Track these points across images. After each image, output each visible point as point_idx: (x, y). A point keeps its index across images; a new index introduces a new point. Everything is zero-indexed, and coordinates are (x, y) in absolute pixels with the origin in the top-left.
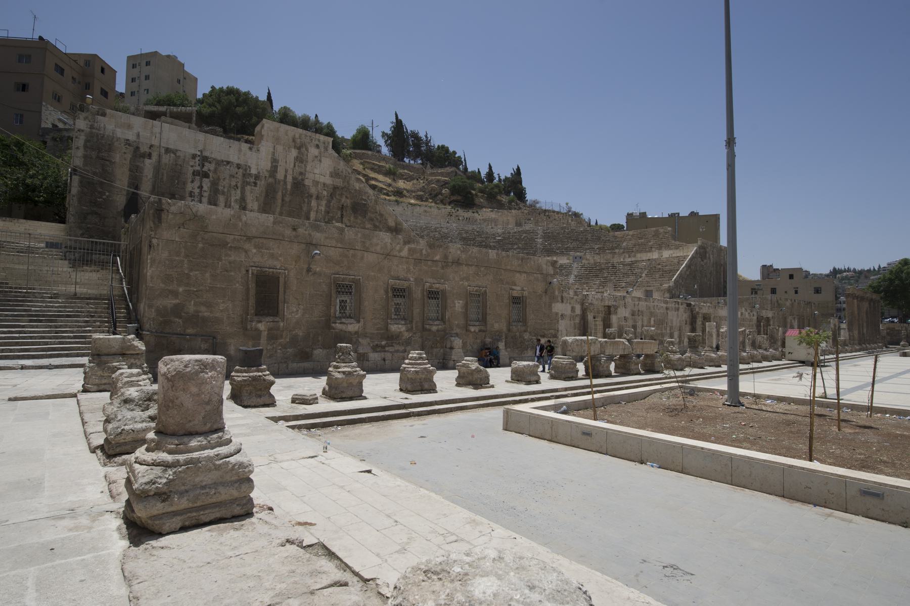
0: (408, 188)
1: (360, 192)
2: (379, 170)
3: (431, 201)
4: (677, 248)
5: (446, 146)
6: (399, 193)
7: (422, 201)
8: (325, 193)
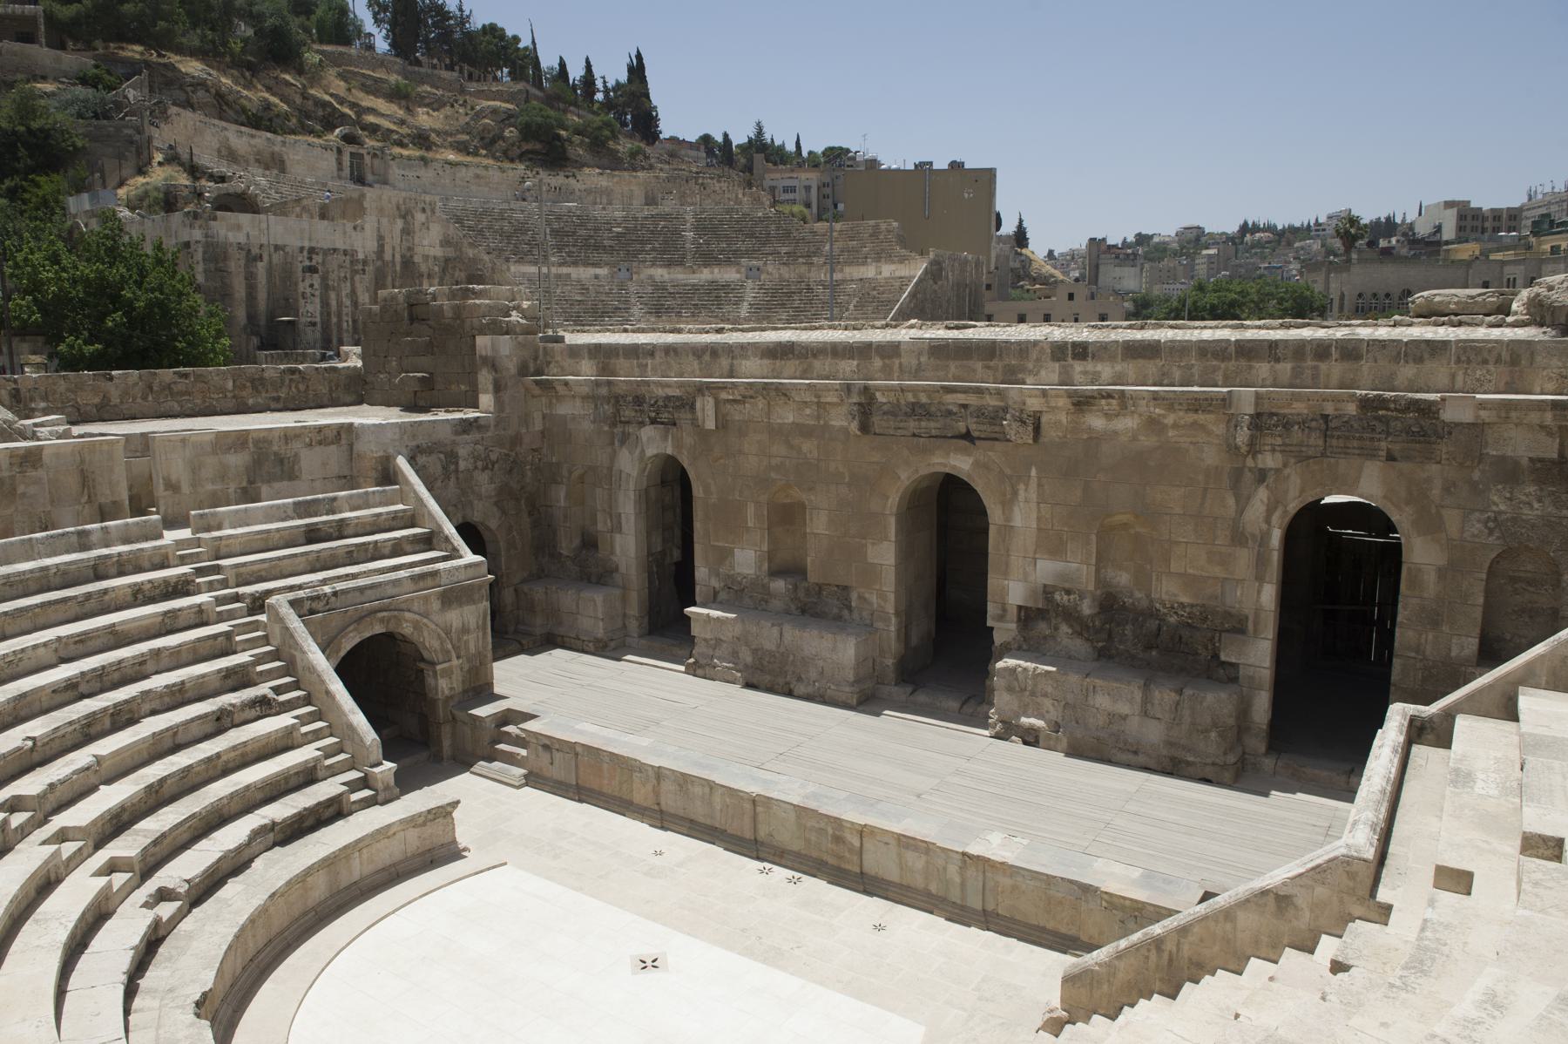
0: (438, 126)
1: (475, 261)
2: (374, 88)
3: (484, 152)
4: (902, 260)
5: (500, 25)
6: (422, 139)
7: (468, 154)
8: (436, 269)
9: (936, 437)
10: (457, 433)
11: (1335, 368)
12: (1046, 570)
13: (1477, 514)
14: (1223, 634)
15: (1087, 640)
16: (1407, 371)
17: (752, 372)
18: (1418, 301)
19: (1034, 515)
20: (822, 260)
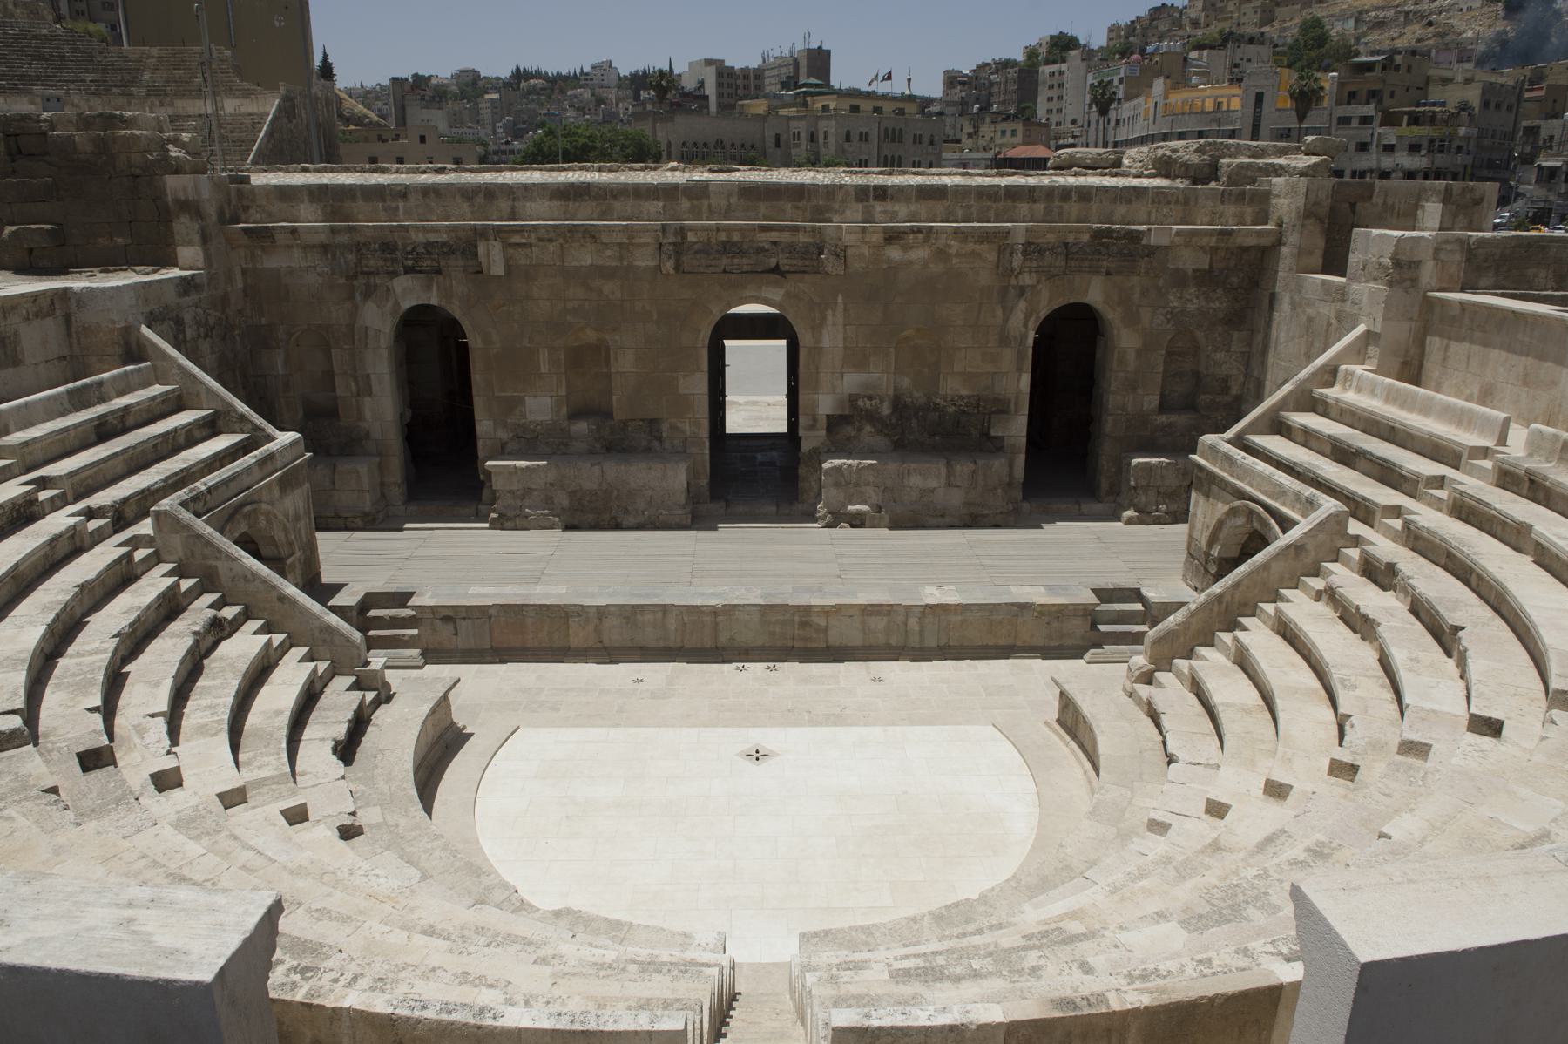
4: (247, 95)
9: (747, 272)
10: (180, 295)
11: (1073, 208)
12: (852, 381)
13: (1161, 310)
14: (993, 416)
15: (886, 435)
16: (1121, 210)
17: (539, 216)
18: (1063, 157)
19: (841, 336)
20: (143, 92)
